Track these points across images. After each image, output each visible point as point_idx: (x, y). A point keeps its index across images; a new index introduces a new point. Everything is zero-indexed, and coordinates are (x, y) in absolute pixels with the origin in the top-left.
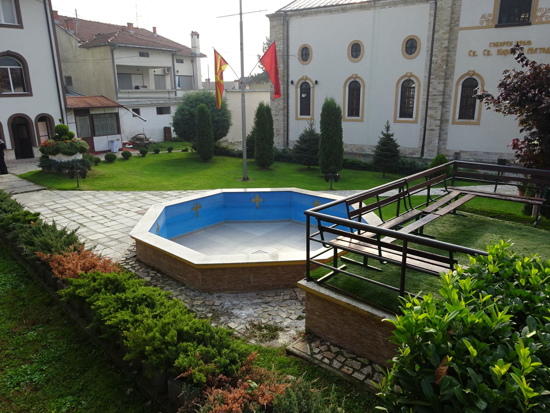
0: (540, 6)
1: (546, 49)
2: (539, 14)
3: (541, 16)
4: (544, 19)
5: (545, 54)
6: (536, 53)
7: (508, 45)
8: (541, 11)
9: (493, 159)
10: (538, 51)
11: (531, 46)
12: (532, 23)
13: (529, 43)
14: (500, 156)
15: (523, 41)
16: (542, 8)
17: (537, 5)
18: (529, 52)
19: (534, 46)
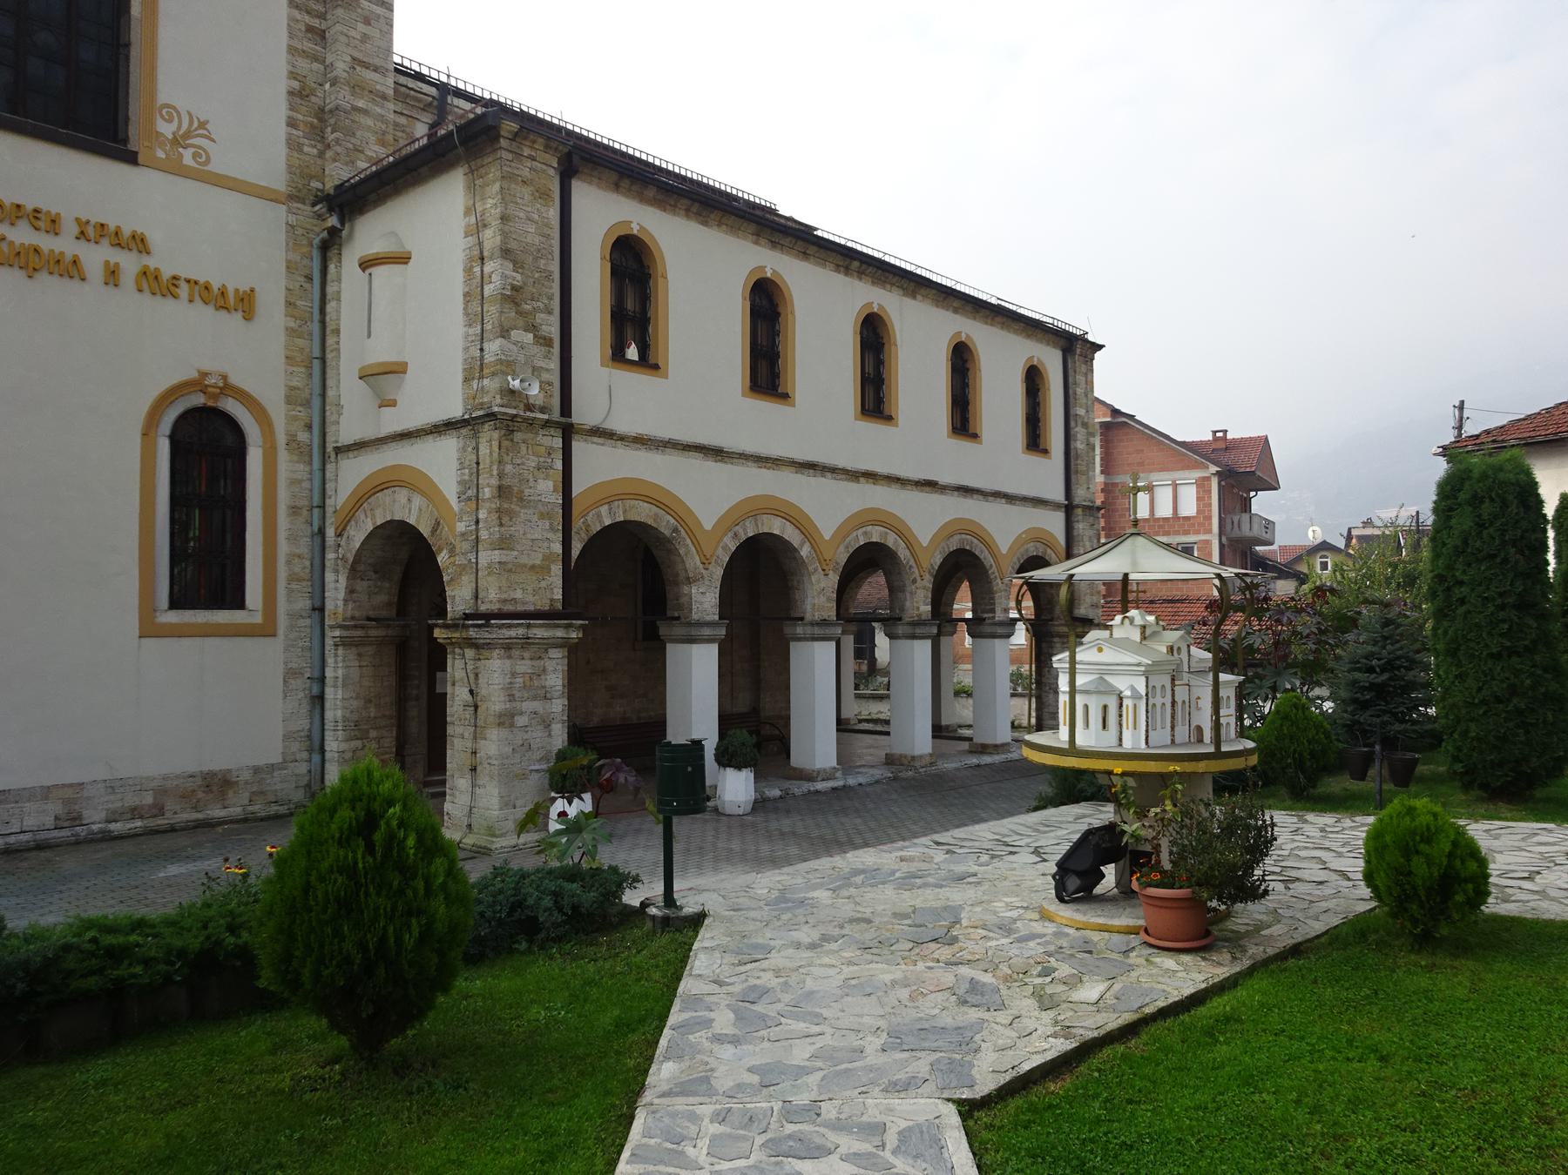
0: (163, 97)
1: (216, 290)
2: (166, 129)
3: (178, 141)
4: (188, 158)
5: (209, 311)
6: (175, 296)
7: (41, 224)
8: (170, 121)
9: (30, 822)
10: (184, 291)
11: (152, 262)
12: (140, 159)
13: (139, 243)
14: (67, 802)
15: (112, 227)
16: (174, 108)
17: (152, 93)
18: (145, 286)
19: (165, 262)
